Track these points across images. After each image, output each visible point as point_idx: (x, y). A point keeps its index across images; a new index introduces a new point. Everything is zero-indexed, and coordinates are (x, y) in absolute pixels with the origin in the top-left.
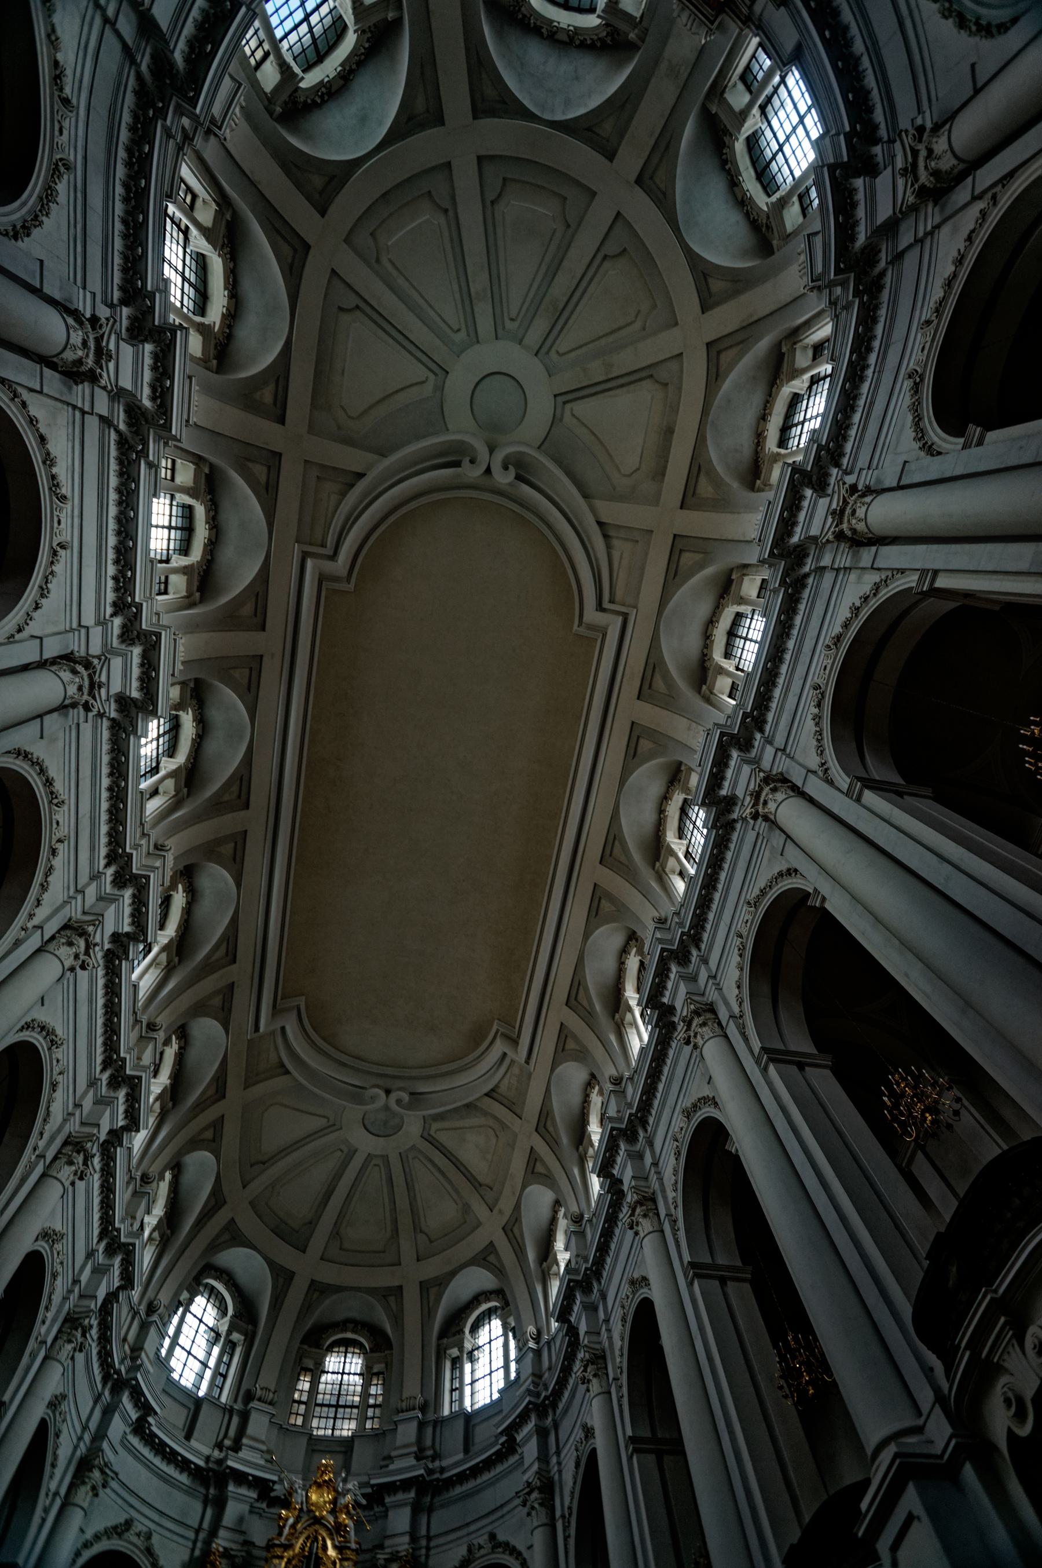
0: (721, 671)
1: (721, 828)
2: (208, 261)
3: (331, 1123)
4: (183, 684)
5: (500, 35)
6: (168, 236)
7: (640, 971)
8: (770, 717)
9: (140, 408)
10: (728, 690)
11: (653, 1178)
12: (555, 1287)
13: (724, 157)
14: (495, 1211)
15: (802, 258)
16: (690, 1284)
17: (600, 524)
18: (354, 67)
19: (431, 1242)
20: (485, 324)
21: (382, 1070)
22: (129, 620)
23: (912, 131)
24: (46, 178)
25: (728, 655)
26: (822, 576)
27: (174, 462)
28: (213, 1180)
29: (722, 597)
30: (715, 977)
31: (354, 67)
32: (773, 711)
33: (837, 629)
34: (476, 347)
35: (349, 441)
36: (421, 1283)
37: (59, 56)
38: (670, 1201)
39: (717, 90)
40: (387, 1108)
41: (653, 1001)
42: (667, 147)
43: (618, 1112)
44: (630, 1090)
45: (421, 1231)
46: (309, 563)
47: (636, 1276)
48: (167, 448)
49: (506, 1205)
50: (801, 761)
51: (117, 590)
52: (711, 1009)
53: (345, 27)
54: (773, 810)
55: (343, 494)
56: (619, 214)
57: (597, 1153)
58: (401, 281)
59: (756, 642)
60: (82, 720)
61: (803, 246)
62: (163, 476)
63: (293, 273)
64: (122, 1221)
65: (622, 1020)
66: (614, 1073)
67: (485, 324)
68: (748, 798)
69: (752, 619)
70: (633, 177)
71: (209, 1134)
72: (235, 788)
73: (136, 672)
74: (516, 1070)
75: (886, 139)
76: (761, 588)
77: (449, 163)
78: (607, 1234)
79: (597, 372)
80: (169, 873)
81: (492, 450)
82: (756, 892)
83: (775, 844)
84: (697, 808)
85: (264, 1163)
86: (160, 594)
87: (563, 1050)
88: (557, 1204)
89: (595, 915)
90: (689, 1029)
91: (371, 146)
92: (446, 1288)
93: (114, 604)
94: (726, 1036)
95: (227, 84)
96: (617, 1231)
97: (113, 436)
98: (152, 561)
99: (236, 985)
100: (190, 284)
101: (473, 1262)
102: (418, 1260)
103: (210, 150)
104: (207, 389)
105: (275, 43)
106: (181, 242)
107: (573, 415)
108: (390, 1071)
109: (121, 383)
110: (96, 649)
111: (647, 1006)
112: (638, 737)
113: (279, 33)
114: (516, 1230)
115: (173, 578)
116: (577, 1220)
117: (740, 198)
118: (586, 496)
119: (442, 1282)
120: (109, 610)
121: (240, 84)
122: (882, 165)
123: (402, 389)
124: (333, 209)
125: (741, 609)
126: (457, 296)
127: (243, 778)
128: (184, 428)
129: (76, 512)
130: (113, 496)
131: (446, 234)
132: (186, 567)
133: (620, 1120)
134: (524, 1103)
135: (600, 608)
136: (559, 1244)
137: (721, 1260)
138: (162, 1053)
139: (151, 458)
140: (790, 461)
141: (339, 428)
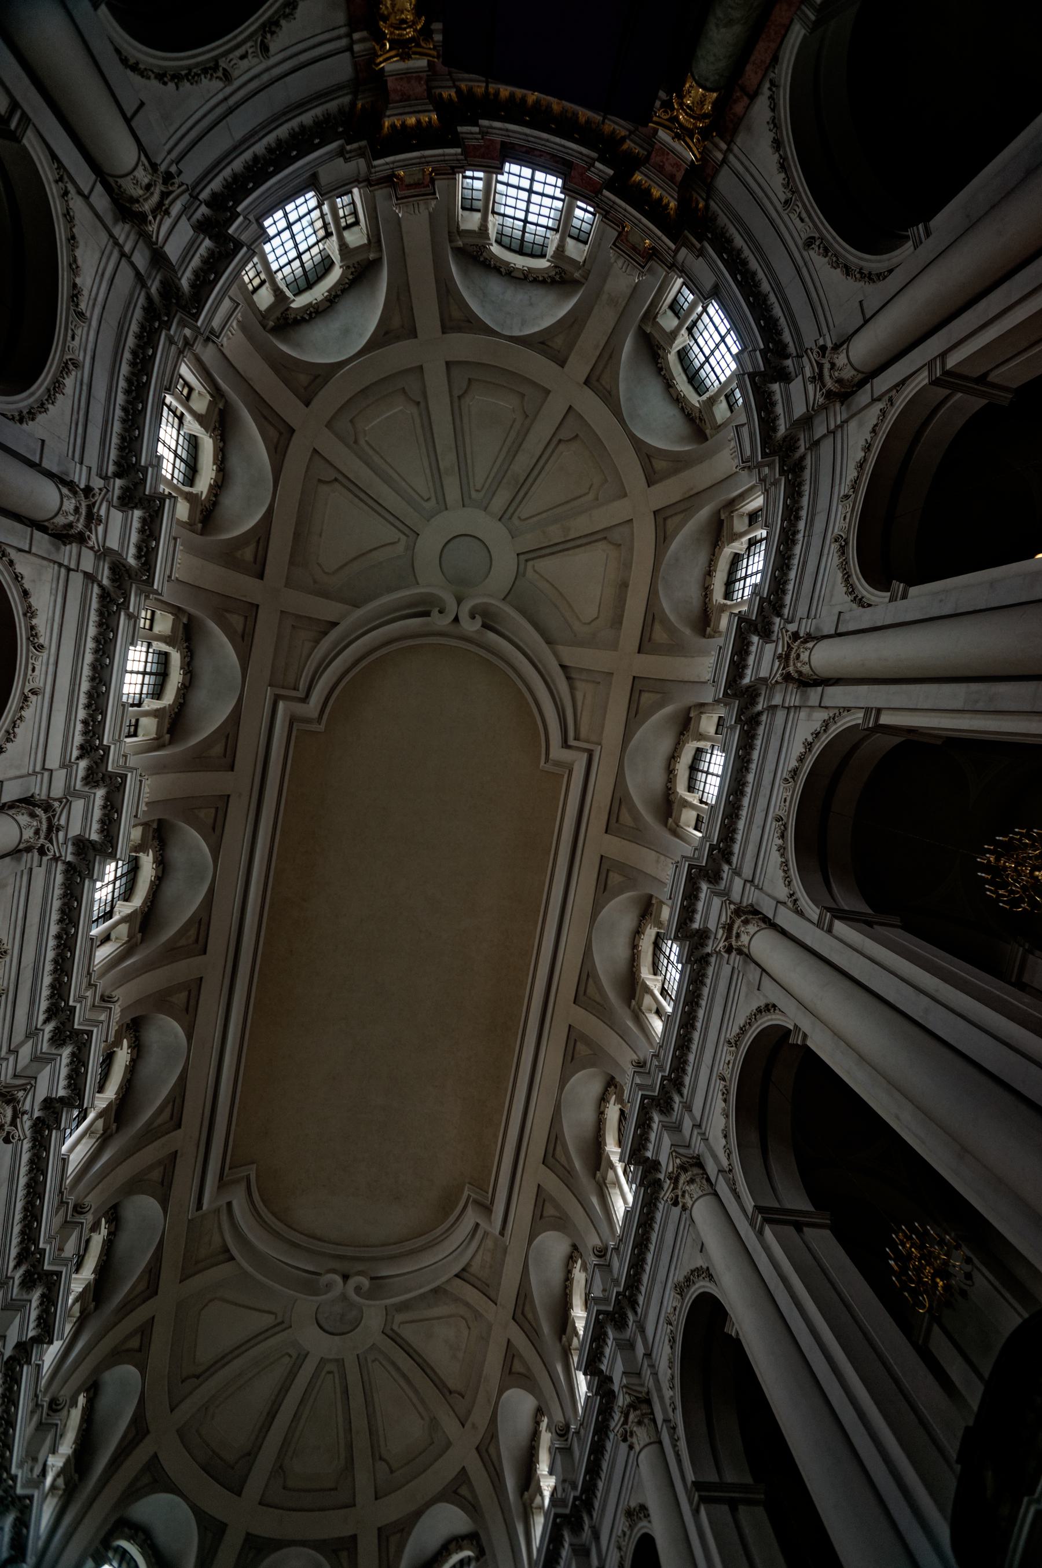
0: (686, 804)
1: (695, 963)
2: (200, 441)
3: (279, 1320)
4: (146, 825)
5: (465, 272)
6: (164, 420)
7: (620, 1121)
8: (736, 848)
9: (124, 566)
10: (693, 823)
11: (647, 1373)
12: (539, 1525)
13: (659, 365)
14: (468, 1425)
15: (733, 444)
16: (696, 1512)
17: (563, 667)
18: (339, 293)
19: (392, 1472)
20: (453, 493)
21: (341, 1251)
22: (96, 763)
23: (816, 350)
24: (54, 374)
25: (691, 788)
26: (774, 714)
27: (153, 613)
28: (136, 1401)
29: (682, 734)
30: (699, 1126)
31: (339, 293)
32: (739, 842)
33: (793, 763)
34: (446, 512)
35: (325, 594)
36: (379, 1529)
37: (78, 281)
38: (668, 1402)
39: (651, 315)
40: (344, 1297)
41: (635, 1156)
42: (610, 357)
43: (604, 1290)
44: (616, 1264)
45: (381, 1458)
46: (281, 705)
47: (633, 1504)
48: (147, 601)
49: (480, 1418)
50: (770, 892)
51: (85, 733)
52: (698, 1163)
53: (332, 263)
54: (746, 943)
55: (317, 642)
56: (570, 406)
57: (582, 1344)
58: (376, 459)
59: (717, 776)
60: (35, 863)
61: (732, 434)
62: (142, 625)
63: (278, 452)
64: (20, 1466)
65: (604, 1179)
66: (597, 1242)
67: (453, 493)
68: (721, 931)
69: (712, 754)
71: (135, 1343)
72: (193, 932)
73: (97, 814)
74: (489, 1243)
75: (795, 354)
76: (718, 725)
77: (421, 367)
78: (598, 1450)
79: (555, 534)
80: (114, 1027)
81: (459, 601)
82: (736, 1030)
83: (751, 977)
84: (670, 942)
85: (198, 1377)
86: (129, 736)
87: (541, 1217)
88: (539, 1412)
89: (571, 1062)
90: (675, 1188)
91: (352, 354)
92: (409, 1534)
93: (82, 747)
94: (716, 1194)
95: (227, 304)
96: (609, 1446)
97: (96, 590)
98: (123, 705)
99: (179, 1154)
100: (182, 460)
101: (441, 1497)
102: (376, 1499)
103: (208, 354)
104: (192, 550)
105: (271, 274)
106: (176, 425)
107: (535, 571)
108: (349, 1252)
109: (108, 544)
110: (57, 791)
111: (629, 1163)
112: (608, 871)
113: (274, 267)
114: (492, 1450)
115: (144, 721)
116: (562, 1432)
117: (675, 397)
118: (549, 642)
119: (405, 1526)
120: (75, 753)
121: (238, 304)
122: (793, 374)
123: (375, 549)
124: (315, 403)
125: (701, 744)
126: (428, 471)
127: (201, 922)
128: (166, 582)
129: (52, 660)
130: (90, 644)
131: (418, 421)
132: (157, 710)
133: (605, 1300)
134: (499, 1284)
135: (566, 745)
136: (543, 1467)
137: (730, 1477)
138: (88, 1241)
139: (131, 610)
140: (736, 611)
141: (315, 582)
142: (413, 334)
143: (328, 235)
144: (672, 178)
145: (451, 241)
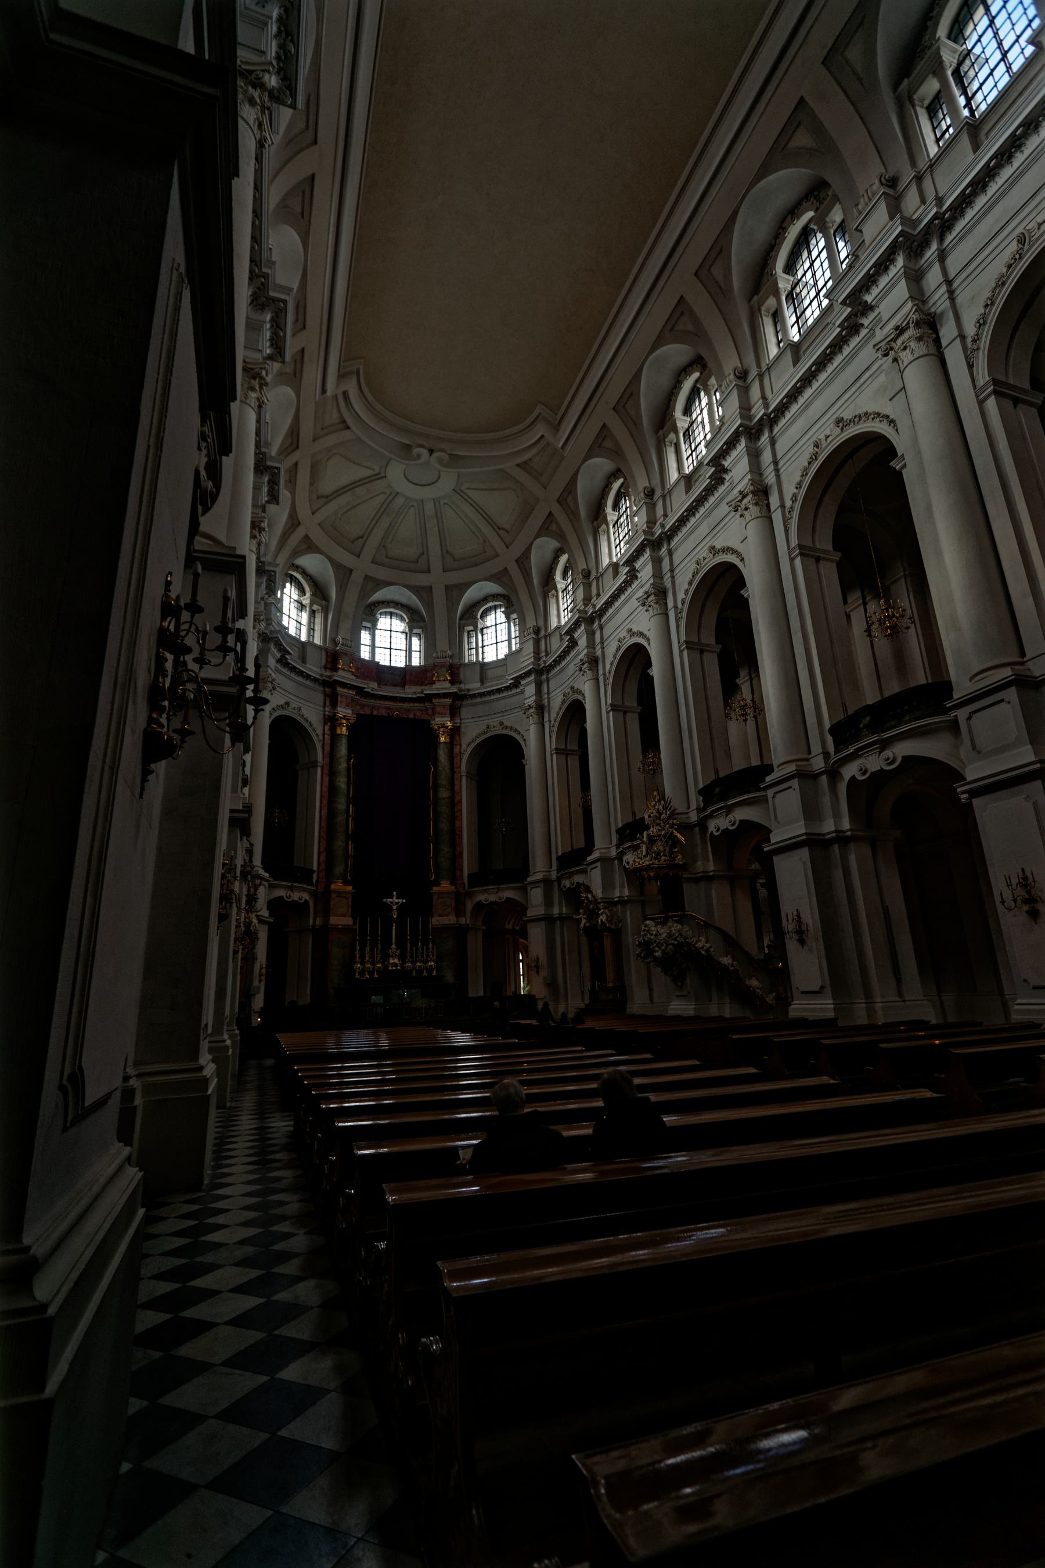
39: (325, 611)
42: (341, 586)
56: (359, 557)
70: (353, 573)
79: (360, 491)
142: (447, 587)
143: (482, 629)
144: (341, 696)
145: (426, 625)
